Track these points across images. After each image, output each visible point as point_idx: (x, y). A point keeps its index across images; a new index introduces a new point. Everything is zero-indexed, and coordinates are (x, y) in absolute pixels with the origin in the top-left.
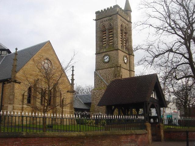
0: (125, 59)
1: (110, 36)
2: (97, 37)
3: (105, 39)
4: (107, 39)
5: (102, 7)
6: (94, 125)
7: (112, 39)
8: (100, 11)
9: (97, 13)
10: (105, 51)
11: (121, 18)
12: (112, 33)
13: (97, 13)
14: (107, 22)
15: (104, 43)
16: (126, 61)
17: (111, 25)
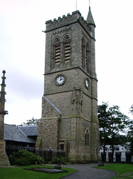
0: (87, 82)
1: (66, 52)
2: (47, 52)
3: (59, 55)
4: (62, 55)
5: (54, 16)
6: (66, 158)
7: (69, 56)
8: (53, 21)
9: (48, 23)
10: (58, 70)
11: (83, 30)
12: (69, 48)
13: (48, 23)
14: (62, 34)
15: (57, 61)
16: (87, 85)
17: (67, 38)
